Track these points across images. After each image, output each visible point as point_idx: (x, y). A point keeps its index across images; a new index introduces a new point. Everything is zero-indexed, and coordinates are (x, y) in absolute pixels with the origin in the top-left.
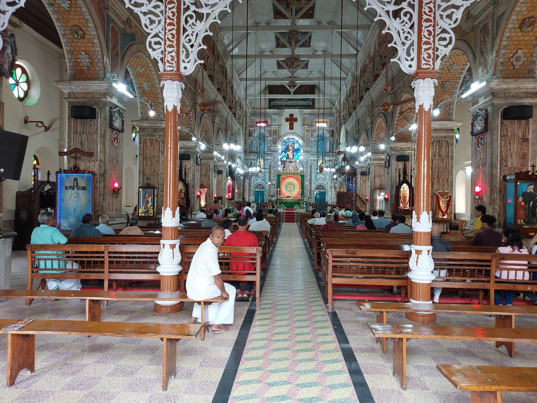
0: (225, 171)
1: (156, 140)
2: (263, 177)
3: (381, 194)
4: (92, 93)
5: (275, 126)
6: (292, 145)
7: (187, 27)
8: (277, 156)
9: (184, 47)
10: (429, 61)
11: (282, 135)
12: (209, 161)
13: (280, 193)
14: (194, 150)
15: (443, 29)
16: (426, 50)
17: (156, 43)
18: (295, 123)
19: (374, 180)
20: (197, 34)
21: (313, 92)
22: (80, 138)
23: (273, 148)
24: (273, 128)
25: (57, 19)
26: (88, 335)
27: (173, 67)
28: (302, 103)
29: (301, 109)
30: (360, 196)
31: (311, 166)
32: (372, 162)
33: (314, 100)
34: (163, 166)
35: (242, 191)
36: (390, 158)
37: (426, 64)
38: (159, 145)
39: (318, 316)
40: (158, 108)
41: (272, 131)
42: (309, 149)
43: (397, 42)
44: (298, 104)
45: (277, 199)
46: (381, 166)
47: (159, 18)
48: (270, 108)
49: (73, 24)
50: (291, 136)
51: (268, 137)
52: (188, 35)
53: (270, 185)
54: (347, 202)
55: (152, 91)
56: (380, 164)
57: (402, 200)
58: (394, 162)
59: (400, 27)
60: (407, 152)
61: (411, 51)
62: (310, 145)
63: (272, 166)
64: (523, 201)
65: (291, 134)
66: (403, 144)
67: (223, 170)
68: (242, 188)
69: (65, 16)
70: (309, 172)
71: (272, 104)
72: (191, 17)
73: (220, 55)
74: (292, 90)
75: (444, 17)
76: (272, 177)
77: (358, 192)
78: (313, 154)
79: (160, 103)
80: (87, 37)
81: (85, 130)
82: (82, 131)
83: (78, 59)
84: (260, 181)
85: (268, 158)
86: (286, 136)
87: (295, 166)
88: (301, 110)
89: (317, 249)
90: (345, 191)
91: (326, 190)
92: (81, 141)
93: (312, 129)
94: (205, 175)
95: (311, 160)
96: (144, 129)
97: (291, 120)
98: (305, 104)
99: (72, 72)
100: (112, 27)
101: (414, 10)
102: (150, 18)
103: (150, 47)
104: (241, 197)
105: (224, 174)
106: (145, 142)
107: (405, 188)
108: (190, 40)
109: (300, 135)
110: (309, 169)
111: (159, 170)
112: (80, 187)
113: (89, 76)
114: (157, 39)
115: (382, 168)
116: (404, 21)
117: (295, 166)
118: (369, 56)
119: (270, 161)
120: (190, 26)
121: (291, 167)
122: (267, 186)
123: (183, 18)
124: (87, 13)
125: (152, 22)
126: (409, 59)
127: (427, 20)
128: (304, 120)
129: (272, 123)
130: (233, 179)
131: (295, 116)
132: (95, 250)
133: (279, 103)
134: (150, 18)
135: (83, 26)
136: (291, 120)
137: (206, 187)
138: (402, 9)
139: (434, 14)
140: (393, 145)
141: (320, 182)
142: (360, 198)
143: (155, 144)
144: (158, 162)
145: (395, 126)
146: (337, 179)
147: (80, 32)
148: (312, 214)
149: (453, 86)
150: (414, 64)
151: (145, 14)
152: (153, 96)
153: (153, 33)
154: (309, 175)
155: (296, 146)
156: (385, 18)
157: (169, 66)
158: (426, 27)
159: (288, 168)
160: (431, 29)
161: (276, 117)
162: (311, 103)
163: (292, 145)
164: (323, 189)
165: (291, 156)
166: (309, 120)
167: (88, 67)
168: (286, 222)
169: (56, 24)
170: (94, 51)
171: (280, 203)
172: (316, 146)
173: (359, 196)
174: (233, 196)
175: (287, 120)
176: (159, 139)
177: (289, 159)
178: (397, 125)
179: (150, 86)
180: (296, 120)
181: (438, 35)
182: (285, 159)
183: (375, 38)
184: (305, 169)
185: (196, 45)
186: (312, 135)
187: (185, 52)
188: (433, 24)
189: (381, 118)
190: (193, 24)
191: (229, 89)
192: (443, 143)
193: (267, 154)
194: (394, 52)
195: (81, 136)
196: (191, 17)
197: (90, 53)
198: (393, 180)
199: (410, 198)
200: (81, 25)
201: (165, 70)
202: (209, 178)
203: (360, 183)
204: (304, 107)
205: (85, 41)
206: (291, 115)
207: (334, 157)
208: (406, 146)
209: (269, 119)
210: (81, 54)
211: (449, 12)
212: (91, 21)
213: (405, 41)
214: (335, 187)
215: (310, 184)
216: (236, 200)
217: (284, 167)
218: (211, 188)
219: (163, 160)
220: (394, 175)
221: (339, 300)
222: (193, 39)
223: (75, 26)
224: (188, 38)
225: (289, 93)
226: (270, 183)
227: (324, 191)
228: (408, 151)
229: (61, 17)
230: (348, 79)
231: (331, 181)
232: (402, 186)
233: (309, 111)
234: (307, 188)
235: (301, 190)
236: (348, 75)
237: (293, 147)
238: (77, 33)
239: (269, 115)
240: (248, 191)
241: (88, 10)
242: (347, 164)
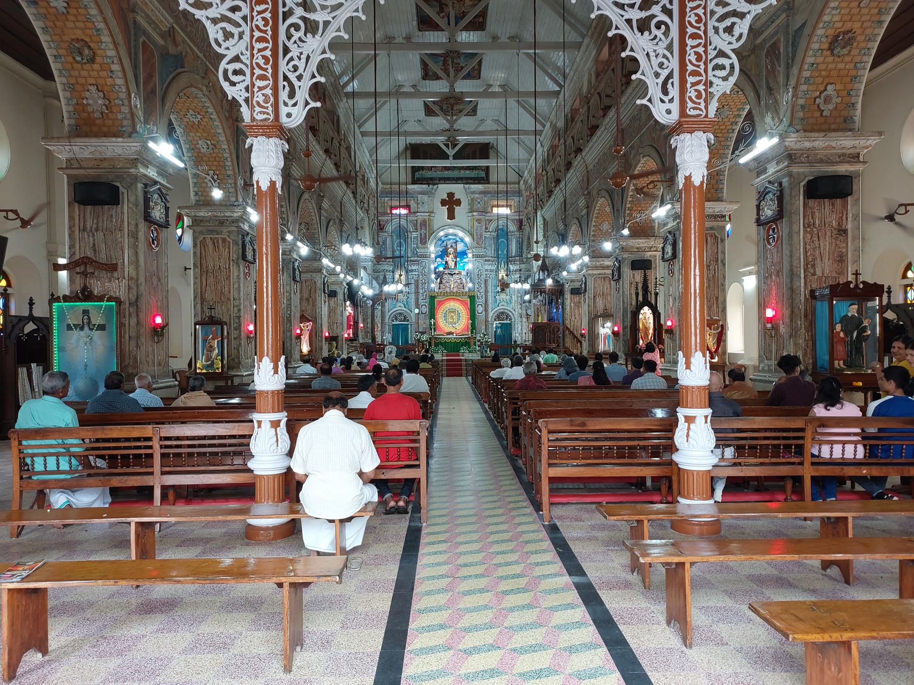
0: (341, 292)
1: (224, 240)
2: (405, 301)
3: (605, 325)
4: (112, 159)
5: (422, 214)
6: (454, 245)
7: (289, 44)
8: (427, 265)
9: (286, 78)
10: (699, 104)
11: (435, 228)
12: (314, 275)
13: (435, 327)
14: (288, 257)
15: (720, 50)
16: (693, 84)
17: (236, 72)
18: (457, 209)
19: (595, 302)
20: (308, 58)
21: (486, 156)
22: (91, 239)
24: (420, 217)
25: (43, 28)
26: (136, 583)
27: (268, 114)
28: (468, 173)
29: (467, 183)
30: (571, 329)
31: (486, 281)
32: (590, 272)
33: (488, 167)
34: (236, 286)
35: (369, 325)
36: (620, 265)
37: (694, 108)
38: (229, 248)
39: (528, 532)
40: (225, 184)
41: (419, 222)
42: (481, 252)
43: (646, 73)
44: (462, 176)
45: (430, 338)
46: (604, 278)
47: (240, 29)
48: (414, 183)
49: (74, 37)
50: (451, 231)
52: (292, 59)
53: (418, 314)
54: (550, 340)
55: (214, 155)
56: (602, 274)
57: (641, 334)
58: (627, 271)
59: (649, 47)
60: (648, 255)
61: (669, 86)
63: (420, 282)
64: (842, 330)
65: (450, 226)
66: (641, 241)
67: (338, 290)
68: (369, 320)
69: (59, 24)
70: (482, 290)
71: (417, 175)
72: (297, 27)
73: (327, 93)
74: (451, 152)
75: (721, 31)
76: (420, 301)
77: (567, 322)
78: (489, 261)
79: (229, 176)
80: (98, 60)
81: (100, 224)
82: (94, 226)
83: (83, 99)
84: (400, 307)
85: (414, 268)
86: (442, 230)
87: (459, 281)
88: (467, 186)
89: (513, 419)
90: (545, 321)
91: (513, 320)
92: (94, 245)
93: (487, 218)
94: (307, 300)
95: (487, 270)
96: (201, 221)
97: (451, 202)
98: (473, 176)
99: (73, 122)
100: (144, 42)
101: (671, 18)
102: (223, 29)
103: (226, 78)
104: (369, 335)
105: (340, 296)
106: (203, 243)
107: (646, 313)
108: (296, 68)
109: (467, 229)
110: (483, 285)
111: (230, 292)
112: (94, 325)
113: (105, 129)
114: (237, 66)
115: (607, 282)
116: (656, 37)
117: (459, 281)
118: (580, 94)
119: (417, 273)
120: (295, 42)
121: (452, 284)
122: (413, 315)
123: (282, 29)
124: (99, 18)
125: (228, 35)
126: (666, 99)
127: (694, 36)
128: (472, 202)
130: (355, 305)
131: (456, 197)
132: (135, 434)
133: (429, 174)
134: (223, 29)
135: (92, 42)
136: (451, 202)
137: (309, 321)
138: (653, 16)
139: (705, 25)
140: (624, 244)
141: (502, 307)
142: (571, 332)
143: (221, 248)
144: (228, 278)
145: (628, 212)
146: (530, 302)
147: (86, 52)
148: (493, 361)
149: (722, 143)
150: (675, 107)
151: (215, 21)
152: (215, 163)
153: (230, 55)
154: (484, 296)
155: (460, 247)
156: (625, 32)
157: (260, 112)
158: (693, 47)
159: (448, 285)
160: (701, 50)
161: (425, 198)
162: (483, 174)
163: (454, 245)
164: (507, 319)
165: (451, 264)
167: (102, 113)
168: (448, 376)
169: (43, 38)
170: (114, 85)
171: (437, 345)
173: (569, 330)
174: (356, 334)
175: (443, 203)
176: (228, 238)
177: (449, 268)
178: (630, 209)
179: (211, 147)
181: (711, 60)
182: (441, 269)
183: (589, 64)
184: (477, 286)
185: (307, 75)
186: (486, 229)
187: (287, 89)
188: (703, 41)
189: (603, 199)
190: (300, 39)
191: (343, 150)
192: (709, 239)
193: (411, 261)
194: (623, 88)
195: (94, 235)
196: (297, 27)
197: (105, 88)
198: (626, 301)
199: (654, 330)
200: (87, 39)
201: (253, 119)
202: (314, 305)
203: (571, 307)
204: (472, 181)
205: (96, 66)
206: (451, 195)
207: (524, 265)
208: (646, 245)
209: (412, 201)
210: (88, 91)
211: (728, 22)
212: (106, 32)
213: (659, 71)
214: (527, 315)
215: (486, 310)
216: (361, 341)
217: (441, 282)
218: (319, 321)
219: (236, 274)
220: (627, 293)
221: (559, 504)
222: (301, 64)
223: (78, 40)
224: (292, 63)
225: (445, 156)
226: (417, 311)
227: (509, 322)
228: (650, 253)
229: (50, 24)
230: (544, 133)
231: (521, 304)
232: (642, 311)
233: (480, 187)
234: (481, 317)
235: (470, 322)
236: (544, 126)
237: (456, 249)
238: (81, 53)
239: (413, 195)
240: (379, 325)
241: (101, 12)
242: (548, 276)
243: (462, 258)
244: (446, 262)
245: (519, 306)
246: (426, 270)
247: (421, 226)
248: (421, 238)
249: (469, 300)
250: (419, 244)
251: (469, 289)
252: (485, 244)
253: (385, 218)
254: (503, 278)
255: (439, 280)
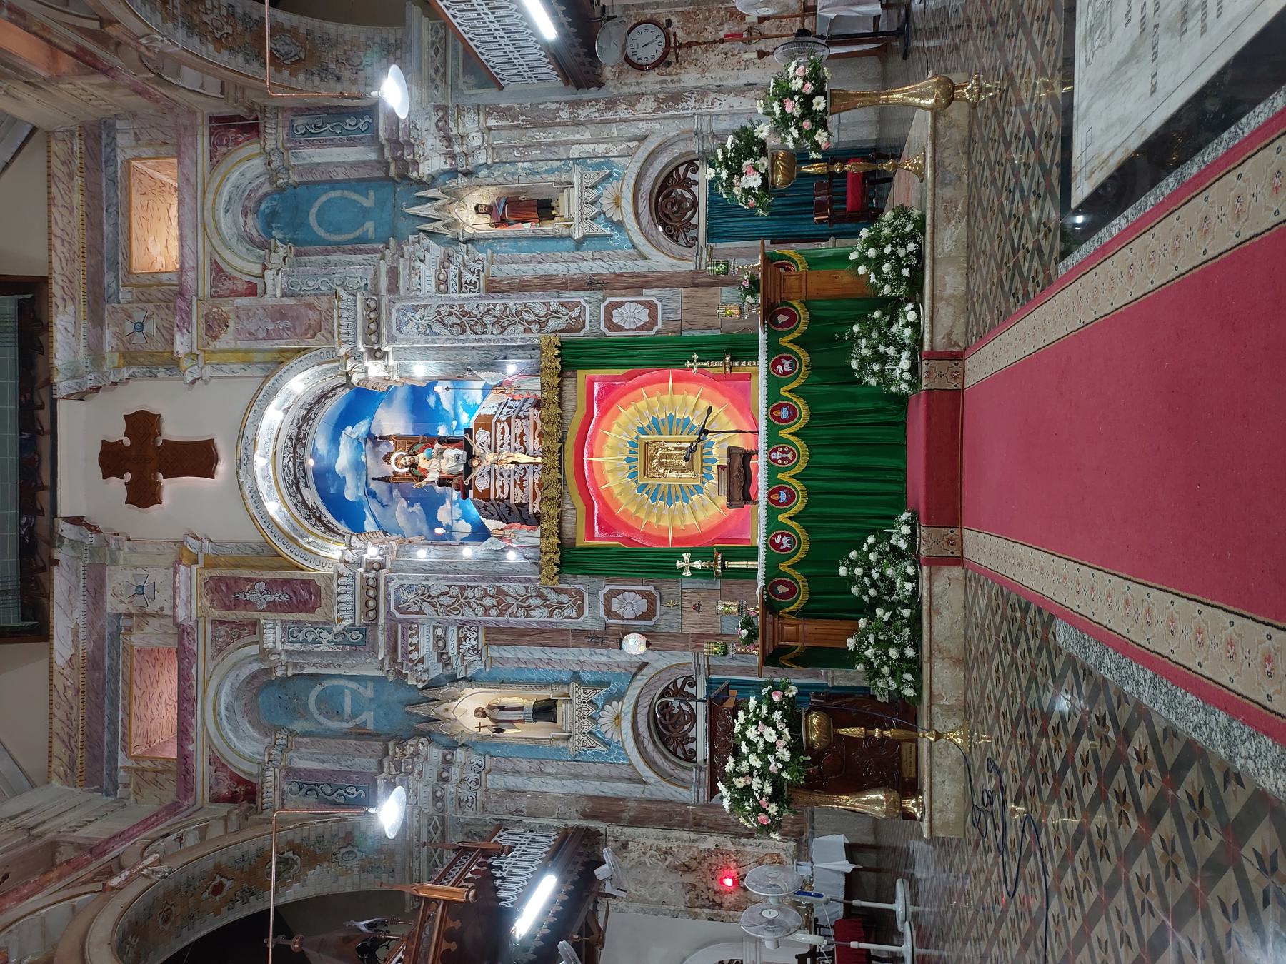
2: (590, 694)
5: (183, 594)
6: (384, 449)
8: (411, 578)
11: (254, 537)
23: (346, 612)
29: (49, 383)
31: (494, 288)
41: (216, 613)
42: (352, 309)
50: (260, 462)
51: (265, 654)
62: (323, 304)
63: (493, 616)
65: (243, 464)
70: (538, 304)
78: (393, 274)
85: (425, 645)
88: (62, 385)
91: (695, 146)
95: (442, 284)
110: (515, 302)
122: (661, 660)
129: (158, 614)
131: (117, 432)
159: (531, 479)
161: (118, 579)
164: (687, 184)
165: (450, 459)
166: (139, 317)
172: (333, 257)
175: (143, 495)
180: (142, 424)
184: (516, 335)
186: (252, 291)
193: (394, 660)
204: (40, 360)
209: (136, 640)
214: (663, 62)
215: (638, 284)
217: (515, 514)
226: (634, 645)
231: (612, 103)
234: (671, 303)
235: (694, 366)
240: (710, 842)
243: (436, 415)
244: (443, 482)
245: (622, 113)
246: (438, 586)
247: (235, 606)
248: (290, 607)
249: (583, 375)
250: (318, 615)
251: (535, 373)
252: (318, 293)
253: (202, 770)
254: (490, 210)
255: (492, 524)
